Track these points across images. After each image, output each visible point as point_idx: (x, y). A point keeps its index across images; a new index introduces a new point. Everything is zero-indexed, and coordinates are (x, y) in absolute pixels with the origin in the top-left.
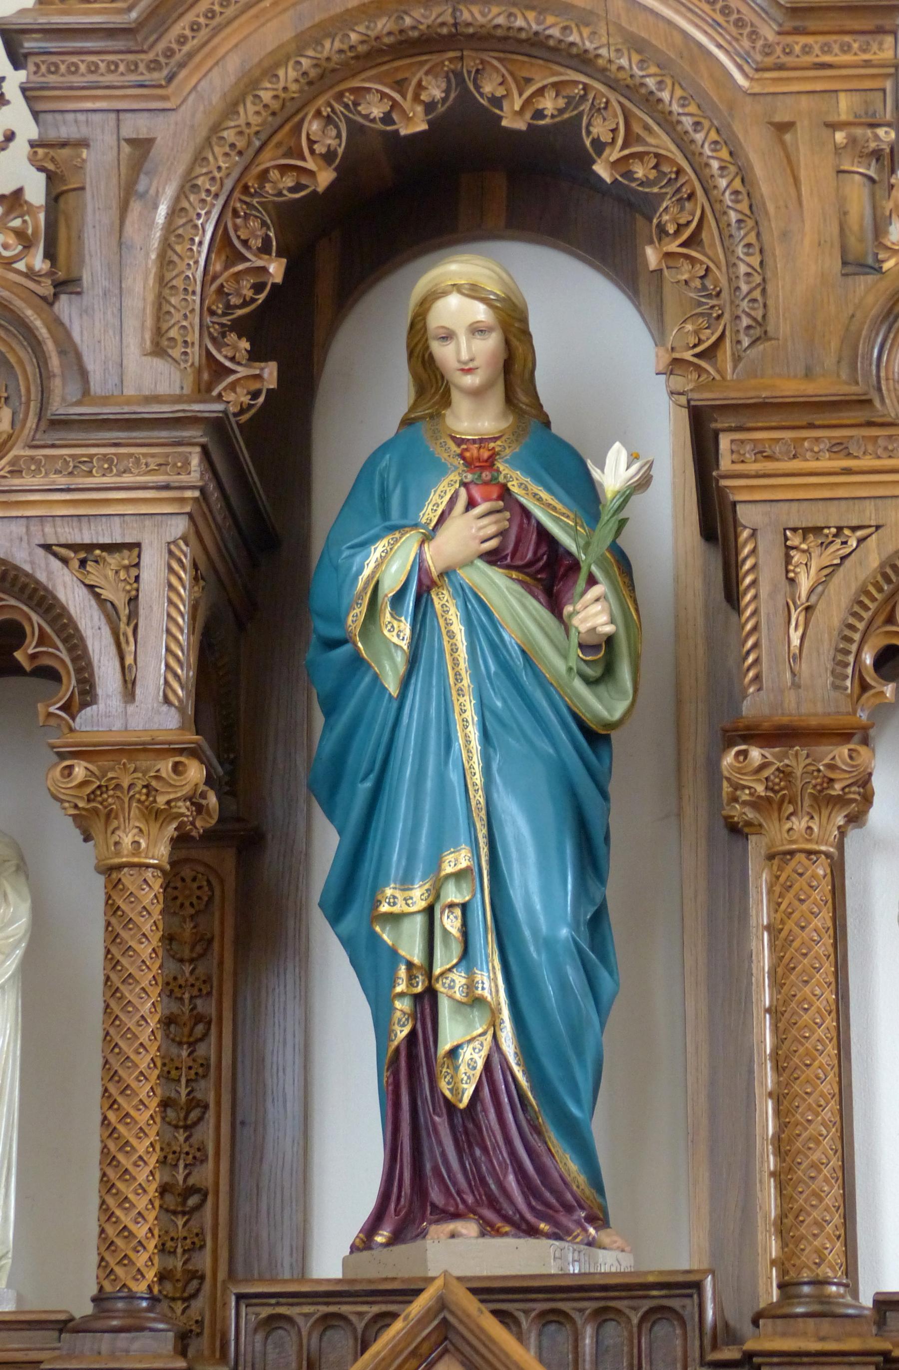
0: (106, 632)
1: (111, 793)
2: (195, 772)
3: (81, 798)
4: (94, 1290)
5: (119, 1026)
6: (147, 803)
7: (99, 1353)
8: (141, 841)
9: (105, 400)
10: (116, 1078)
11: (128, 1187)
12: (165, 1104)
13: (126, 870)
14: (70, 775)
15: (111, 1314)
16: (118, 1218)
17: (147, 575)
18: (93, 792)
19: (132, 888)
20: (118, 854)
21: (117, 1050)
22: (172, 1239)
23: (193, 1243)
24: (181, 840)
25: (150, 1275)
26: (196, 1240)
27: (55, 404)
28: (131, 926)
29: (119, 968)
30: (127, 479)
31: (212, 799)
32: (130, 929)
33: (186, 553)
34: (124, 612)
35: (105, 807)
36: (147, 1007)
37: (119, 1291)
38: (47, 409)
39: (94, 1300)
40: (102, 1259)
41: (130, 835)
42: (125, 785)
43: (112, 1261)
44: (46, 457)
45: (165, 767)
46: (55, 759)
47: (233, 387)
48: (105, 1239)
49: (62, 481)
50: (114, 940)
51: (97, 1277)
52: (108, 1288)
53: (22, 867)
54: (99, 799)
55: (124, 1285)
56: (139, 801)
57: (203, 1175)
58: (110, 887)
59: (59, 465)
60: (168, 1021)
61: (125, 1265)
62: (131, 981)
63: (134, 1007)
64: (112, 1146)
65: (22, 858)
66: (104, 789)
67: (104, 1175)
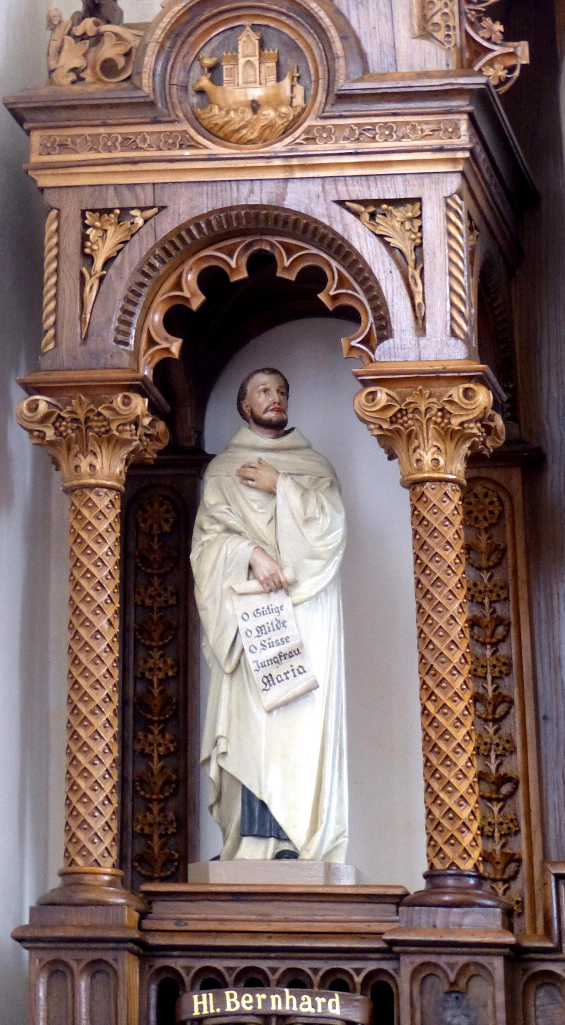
0: (397, 274)
1: (410, 416)
2: (483, 397)
3: (385, 420)
4: (425, 868)
5: (431, 625)
6: (442, 425)
7: (435, 926)
8: (440, 458)
9: (382, 77)
10: (432, 672)
11: (450, 771)
12: (477, 698)
13: (428, 484)
14: (373, 400)
15: (443, 890)
16: (442, 800)
17: (427, 226)
18: (395, 415)
19: (435, 501)
20: (420, 470)
21: (431, 646)
22: (490, 824)
23: (509, 828)
24: (474, 460)
25: (476, 854)
26: (511, 825)
27: (341, 81)
28: (436, 534)
29: (428, 572)
30: (406, 143)
31: (499, 422)
32: (436, 537)
33: (462, 206)
34: (411, 258)
35: (407, 429)
36: (455, 610)
37: (449, 868)
38: (334, 85)
39: (426, 876)
40: (431, 838)
41: (429, 453)
42: (423, 409)
43: (440, 841)
44: (335, 126)
45: (457, 392)
46: (360, 386)
47: (490, 63)
48: (432, 820)
49: (350, 146)
50: (422, 547)
51: (428, 856)
52: (438, 866)
53: (336, 484)
54: (400, 421)
55: (453, 864)
56: (435, 423)
57: (513, 766)
58: (415, 499)
59: (347, 133)
60: (473, 623)
61: (452, 845)
62: (439, 584)
63: (444, 607)
64: (433, 735)
65: (335, 476)
66: (404, 412)
67: (427, 760)
